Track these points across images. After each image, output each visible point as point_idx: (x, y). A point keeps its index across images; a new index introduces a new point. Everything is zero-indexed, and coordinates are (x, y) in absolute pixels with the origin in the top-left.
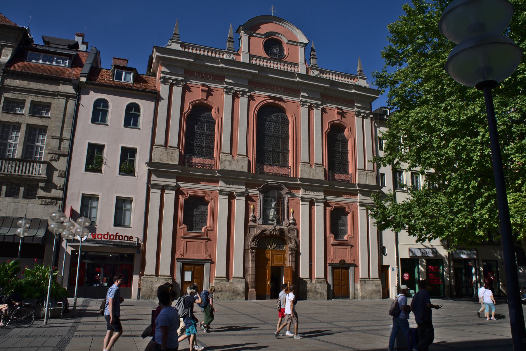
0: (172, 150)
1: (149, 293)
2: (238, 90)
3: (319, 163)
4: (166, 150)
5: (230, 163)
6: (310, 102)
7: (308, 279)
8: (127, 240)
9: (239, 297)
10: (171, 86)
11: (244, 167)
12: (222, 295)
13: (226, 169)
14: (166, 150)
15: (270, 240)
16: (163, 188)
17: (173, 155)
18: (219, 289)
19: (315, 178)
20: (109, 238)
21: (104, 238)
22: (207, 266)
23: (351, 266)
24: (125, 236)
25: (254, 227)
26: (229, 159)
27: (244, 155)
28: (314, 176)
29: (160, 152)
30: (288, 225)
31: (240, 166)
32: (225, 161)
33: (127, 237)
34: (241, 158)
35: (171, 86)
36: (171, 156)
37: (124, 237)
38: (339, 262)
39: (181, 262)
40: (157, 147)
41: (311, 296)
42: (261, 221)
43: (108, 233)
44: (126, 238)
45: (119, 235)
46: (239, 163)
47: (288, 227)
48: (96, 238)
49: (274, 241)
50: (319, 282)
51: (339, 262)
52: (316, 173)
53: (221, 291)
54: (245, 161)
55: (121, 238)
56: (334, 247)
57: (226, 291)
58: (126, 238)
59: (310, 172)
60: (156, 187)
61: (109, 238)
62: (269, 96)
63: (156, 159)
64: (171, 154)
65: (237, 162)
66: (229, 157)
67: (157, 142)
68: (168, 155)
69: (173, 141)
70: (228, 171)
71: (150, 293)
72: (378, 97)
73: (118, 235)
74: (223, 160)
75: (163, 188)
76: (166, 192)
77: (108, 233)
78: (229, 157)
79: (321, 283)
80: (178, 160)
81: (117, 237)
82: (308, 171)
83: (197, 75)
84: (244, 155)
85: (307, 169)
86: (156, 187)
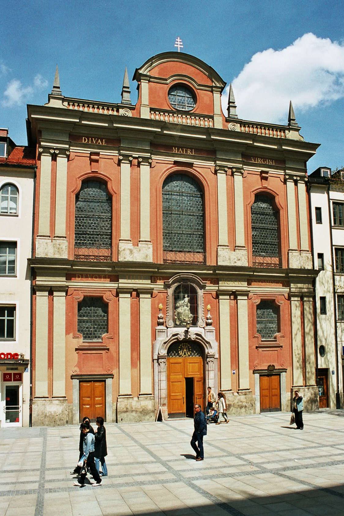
0: (58, 241)
1: (42, 419)
2: (137, 156)
3: (242, 245)
4: (52, 242)
5: (131, 251)
6: (229, 166)
7: (231, 390)
9: (148, 417)
11: (148, 257)
12: (127, 415)
14: (52, 242)
16: (51, 288)
17: (61, 246)
18: (125, 409)
19: (236, 265)
22: (109, 381)
23: (282, 372)
25: (164, 331)
26: (130, 248)
27: (148, 241)
28: (235, 262)
29: (44, 244)
31: (144, 256)
32: (124, 250)
39: (78, 379)
40: (40, 238)
41: (233, 411)
42: (171, 323)
46: (141, 252)
47: (204, 328)
49: (188, 347)
50: (243, 393)
51: (266, 368)
52: (237, 258)
53: (127, 411)
54: (149, 248)
56: (260, 349)
57: (132, 411)
60: (42, 288)
62: (176, 163)
63: (40, 254)
66: (130, 246)
71: (44, 418)
72: (315, 154)
74: (123, 248)
75: (51, 288)
76: (55, 294)
79: (245, 394)
80: (67, 252)
83: (85, 140)
84: (148, 241)
85: (227, 253)
86: (42, 288)
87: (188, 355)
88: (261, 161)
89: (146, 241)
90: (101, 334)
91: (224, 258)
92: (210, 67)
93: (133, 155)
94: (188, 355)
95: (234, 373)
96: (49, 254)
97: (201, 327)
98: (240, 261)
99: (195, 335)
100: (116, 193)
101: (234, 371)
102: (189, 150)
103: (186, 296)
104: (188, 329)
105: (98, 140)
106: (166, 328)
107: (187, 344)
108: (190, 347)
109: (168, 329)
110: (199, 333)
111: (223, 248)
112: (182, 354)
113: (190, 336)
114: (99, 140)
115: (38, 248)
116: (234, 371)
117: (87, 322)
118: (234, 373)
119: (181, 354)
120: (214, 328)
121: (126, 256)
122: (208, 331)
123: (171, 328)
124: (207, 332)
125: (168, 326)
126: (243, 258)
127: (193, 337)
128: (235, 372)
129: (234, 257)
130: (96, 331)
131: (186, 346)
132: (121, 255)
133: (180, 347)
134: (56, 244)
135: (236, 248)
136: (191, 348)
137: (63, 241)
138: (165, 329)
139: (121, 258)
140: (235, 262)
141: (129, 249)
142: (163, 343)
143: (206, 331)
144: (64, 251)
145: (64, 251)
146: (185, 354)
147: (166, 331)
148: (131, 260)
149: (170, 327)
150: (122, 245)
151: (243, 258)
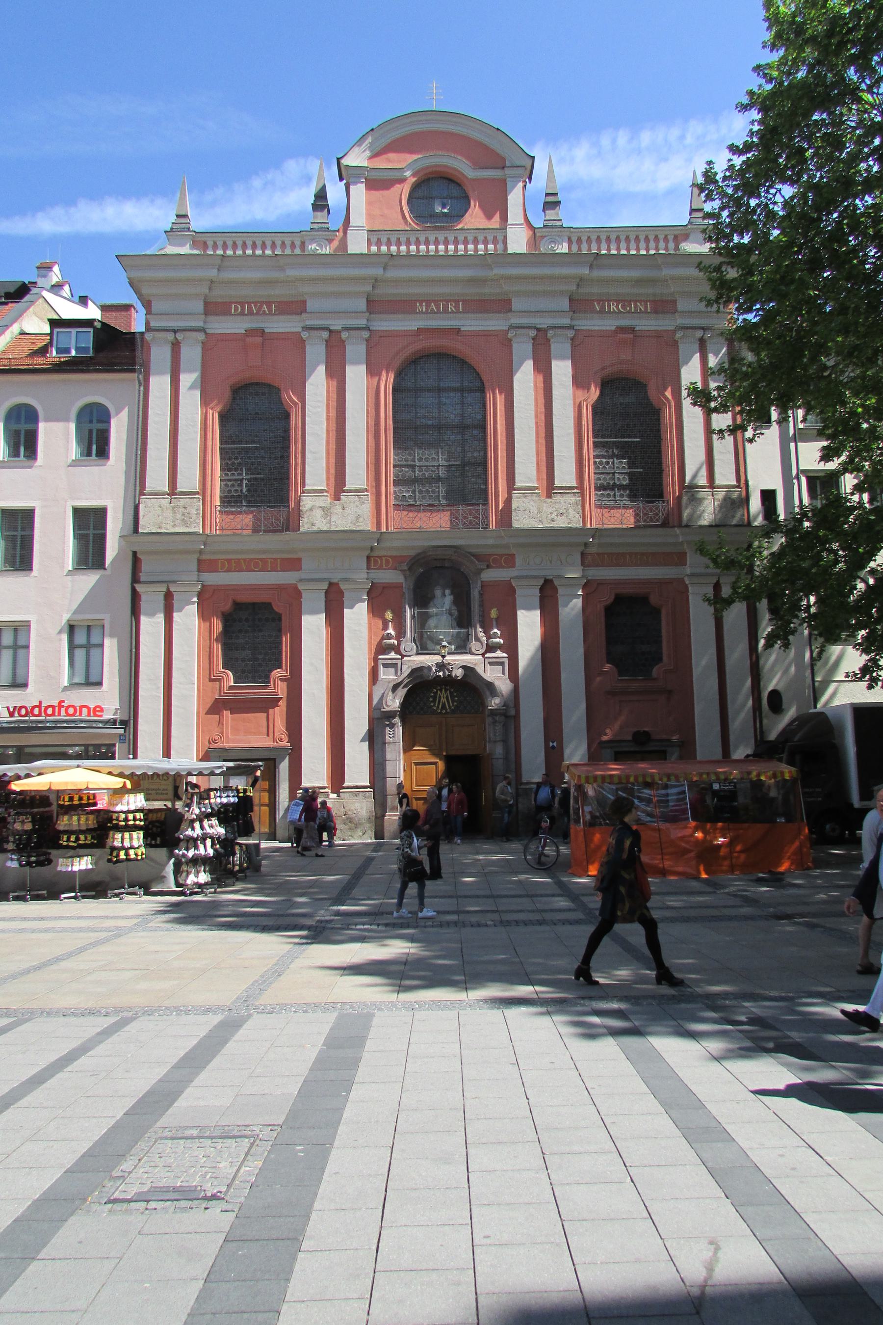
0: (183, 501)
2: (339, 328)
5: (326, 511)
6: (538, 326)
8: (89, 715)
10: (176, 346)
11: (362, 520)
13: (315, 528)
15: (441, 692)
19: (554, 525)
20: (57, 714)
21: (68, 714)
24: (81, 707)
28: (553, 520)
29: (157, 508)
30: (482, 651)
32: (311, 510)
33: (86, 707)
34: (352, 499)
35: (176, 346)
36: (183, 515)
37: (78, 708)
38: (630, 738)
43: (40, 702)
44: (85, 711)
45: (65, 705)
46: (348, 511)
47: (483, 655)
48: (16, 714)
49: (451, 693)
54: (363, 503)
55: (71, 711)
58: (85, 711)
59: (539, 511)
61: (57, 714)
64: (182, 510)
65: (344, 508)
67: (150, 486)
68: (174, 512)
69: (189, 478)
73: (63, 706)
74: (308, 507)
77: (40, 702)
81: (63, 710)
83: (236, 309)
85: (532, 503)
88: (617, 307)
89: (357, 491)
90: (271, 671)
91: (527, 512)
92: (498, 129)
93: (332, 328)
96: (164, 525)
97: (476, 652)
99: (460, 670)
100: (296, 404)
101: (553, 742)
102: (451, 305)
103: (447, 592)
104: (443, 657)
105: (261, 307)
106: (400, 657)
107: (448, 687)
109: (405, 658)
114: (265, 306)
115: (144, 516)
116: (553, 742)
117: (243, 649)
118: (553, 747)
119: (435, 708)
120: (506, 655)
122: (491, 660)
124: (489, 663)
125: (404, 653)
126: (571, 511)
127: (459, 673)
128: (555, 744)
129: (550, 510)
130: (260, 665)
131: (446, 692)
132: (305, 520)
134: (178, 506)
135: (551, 489)
136: (456, 696)
137: (191, 500)
139: (305, 526)
140: (553, 520)
142: (391, 685)
144: (194, 519)
145: (194, 519)
146: (444, 707)
147: (399, 662)
149: (408, 654)
150: (307, 502)
151: (571, 511)
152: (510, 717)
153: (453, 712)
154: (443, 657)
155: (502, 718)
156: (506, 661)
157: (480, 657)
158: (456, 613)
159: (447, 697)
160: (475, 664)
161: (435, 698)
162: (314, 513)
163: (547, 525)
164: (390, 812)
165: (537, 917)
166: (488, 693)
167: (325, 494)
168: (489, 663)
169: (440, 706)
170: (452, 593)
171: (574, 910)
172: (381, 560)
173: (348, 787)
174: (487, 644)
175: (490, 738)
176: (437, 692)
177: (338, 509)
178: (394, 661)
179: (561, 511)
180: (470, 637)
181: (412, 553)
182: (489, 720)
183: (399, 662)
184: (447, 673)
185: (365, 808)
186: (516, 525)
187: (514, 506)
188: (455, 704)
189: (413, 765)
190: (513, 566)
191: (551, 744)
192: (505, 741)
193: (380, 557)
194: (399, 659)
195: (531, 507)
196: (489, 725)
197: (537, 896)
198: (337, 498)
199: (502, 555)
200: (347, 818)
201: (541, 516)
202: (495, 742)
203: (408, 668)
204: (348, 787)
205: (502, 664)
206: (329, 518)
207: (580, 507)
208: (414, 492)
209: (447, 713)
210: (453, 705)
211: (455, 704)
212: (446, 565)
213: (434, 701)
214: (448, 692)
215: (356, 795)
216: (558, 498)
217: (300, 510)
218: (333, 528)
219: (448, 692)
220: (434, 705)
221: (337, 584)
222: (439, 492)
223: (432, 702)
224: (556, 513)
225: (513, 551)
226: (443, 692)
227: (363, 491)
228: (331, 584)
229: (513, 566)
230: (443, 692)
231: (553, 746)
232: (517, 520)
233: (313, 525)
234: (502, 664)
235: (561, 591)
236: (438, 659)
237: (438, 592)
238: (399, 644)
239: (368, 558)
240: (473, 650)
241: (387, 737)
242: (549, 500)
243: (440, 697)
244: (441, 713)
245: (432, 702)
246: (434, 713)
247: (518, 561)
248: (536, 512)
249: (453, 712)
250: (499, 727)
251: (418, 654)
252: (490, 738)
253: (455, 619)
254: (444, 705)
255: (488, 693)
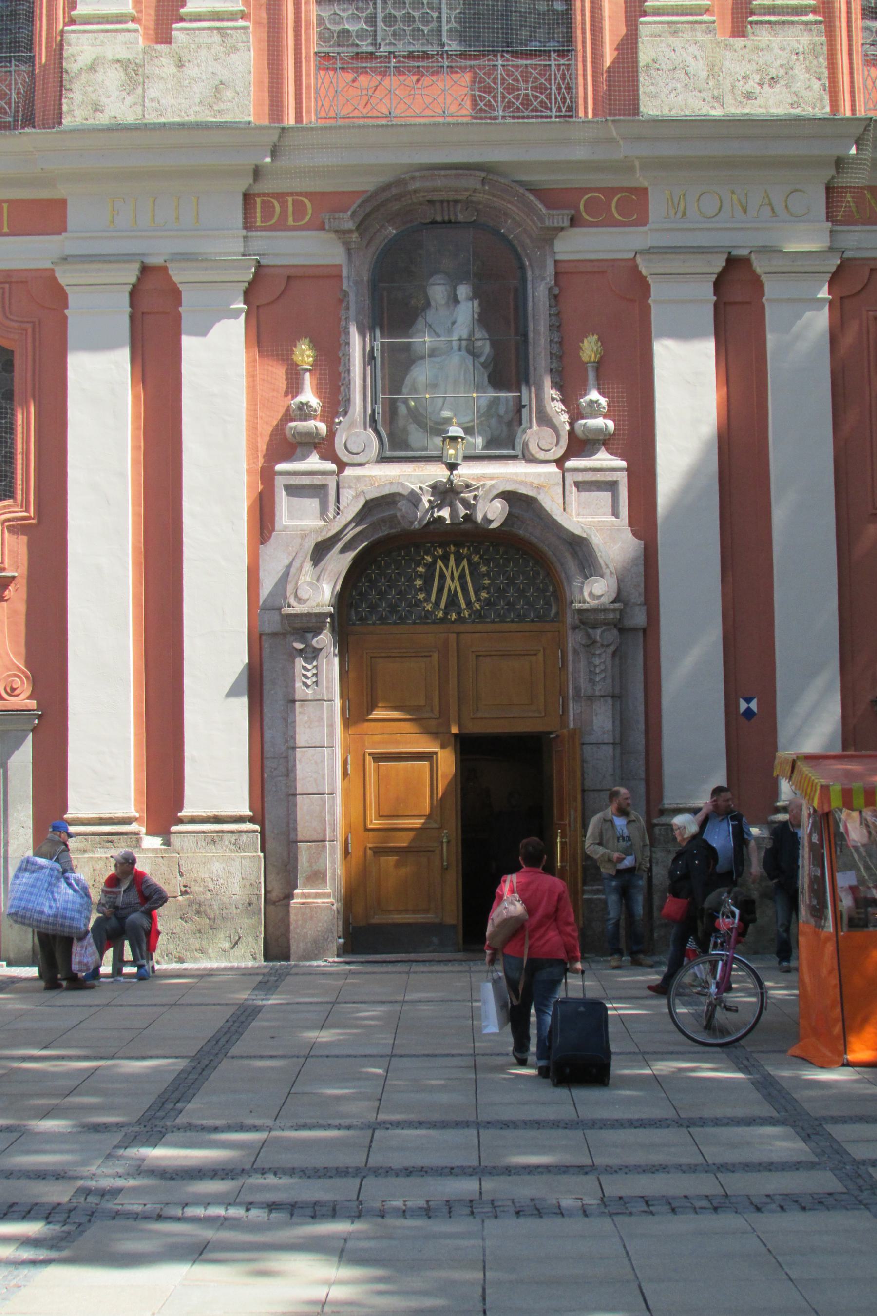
11: (229, 94)
13: (103, 119)
28: (749, 96)
30: (559, 452)
32: (92, 68)
34: (204, 38)
46: (192, 71)
47: (560, 462)
49: (473, 567)
54: (235, 49)
59: (713, 70)
65: (180, 64)
70: (117, 128)
78: (121, 37)
82: (699, 68)
85: (693, 49)
87: (473, 612)
89: (217, 16)
91: (680, 74)
94: (473, 612)
95: (749, 713)
97: (541, 455)
98: (777, 88)
101: (748, 700)
103: (463, 291)
104: (452, 467)
106: (333, 467)
108: (484, 569)
109: (349, 472)
110: (523, 490)
111: (668, 23)
112: (437, 604)
113: (466, 503)
116: (748, 700)
118: (749, 713)
119: (429, 607)
120: (623, 464)
121: (104, 100)
122: (580, 477)
123: (360, 465)
124: (577, 484)
125: (345, 457)
126: (800, 73)
128: (754, 705)
133: (421, 569)
136: (487, 574)
138: (324, 473)
140: (749, 96)
141: (118, 61)
142: (310, 544)
143: (570, 478)
147: (331, 482)
148: (130, 117)
149: (357, 459)
151: (800, 73)
152: (634, 630)
153: (479, 617)
154: (452, 467)
155: (612, 635)
156: (622, 478)
157: (553, 469)
158: (486, 349)
159: (462, 577)
160: (539, 488)
161: (428, 580)
162: (100, 76)
163: (733, 108)
164: (305, 886)
165: (705, 1185)
166: (572, 566)
167: (131, 26)
168: (577, 484)
169: (442, 605)
170: (476, 294)
171: (811, 1166)
172: (284, 205)
173: (193, 820)
174: (571, 433)
175: (577, 690)
176: (434, 562)
177: (165, 66)
178: (317, 480)
179: (773, 73)
180: (525, 412)
181: (368, 184)
182: (574, 640)
183: (331, 482)
184: (462, 511)
185: (238, 876)
186: (649, 108)
187: (644, 58)
188: (484, 595)
189: (369, 759)
190: (643, 221)
191: (743, 706)
192: (618, 697)
193: (280, 196)
194: (331, 473)
195: (690, 60)
196: (575, 652)
197: (703, 1122)
198: (163, 36)
199: (610, 192)
200: (190, 903)
201: (718, 85)
202: (591, 698)
203: (357, 496)
204: (193, 820)
205: (612, 486)
206: (139, 90)
207: (823, 61)
208: (372, 20)
209: (461, 620)
210: (478, 600)
211: (484, 595)
212: (460, 218)
213: (427, 587)
214: (465, 563)
215: (214, 839)
216: (763, 37)
217: (61, 71)
218: (152, 118)
219: (465, 563)
220: (427, 600)
221: (163, 269)
222: (439, 18)
223: (421, 589)
224: (757, 78)
225: (640, 179)
226: (452, 562)
227: (231, 17)
228: (145, 269)
229: (643, 221)
230: (452, 562)
231: (749, 709)
232: (655, 96)
233: (97, 108)
234: (612, 486)
235: (772, 289)
236: (437, 473)
237: (438, 292)
238: (332, 433)
239: (248, 198)
240: (533, 448)
241: (298, 685)
242: (739, 42)
243: (442, 576)
244: (443, 620)
245: (421, 589)
246: (426, 618)
247: (657, 207)
248: (704, 74)
249: (479, 617)
250: (602, 660)
251: (383, 459)
252: (577, 690)
253: (484, 365)
254: (453, 598)
255: (572, 566)
